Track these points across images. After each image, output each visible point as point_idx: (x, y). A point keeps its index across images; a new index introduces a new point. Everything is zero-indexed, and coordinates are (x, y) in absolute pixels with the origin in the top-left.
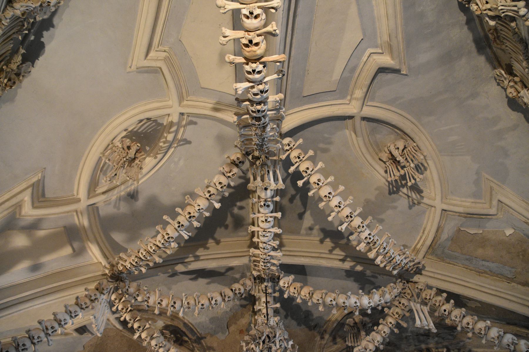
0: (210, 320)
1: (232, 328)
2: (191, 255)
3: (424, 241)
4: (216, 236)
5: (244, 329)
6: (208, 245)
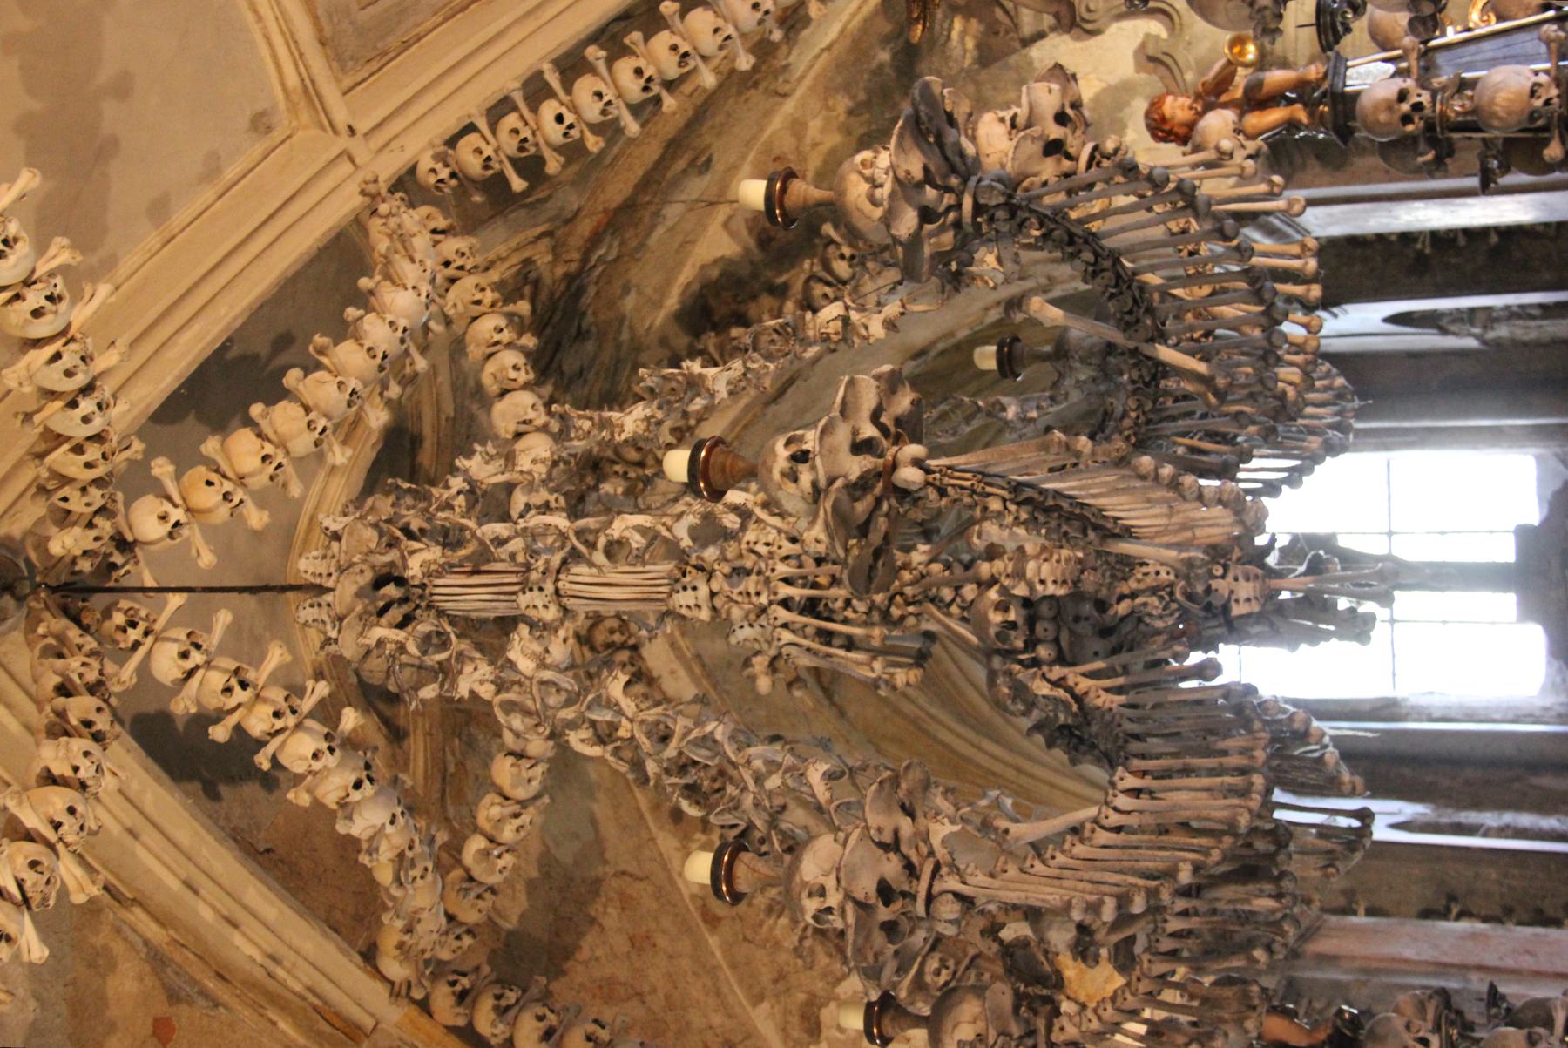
3: (292, 40)
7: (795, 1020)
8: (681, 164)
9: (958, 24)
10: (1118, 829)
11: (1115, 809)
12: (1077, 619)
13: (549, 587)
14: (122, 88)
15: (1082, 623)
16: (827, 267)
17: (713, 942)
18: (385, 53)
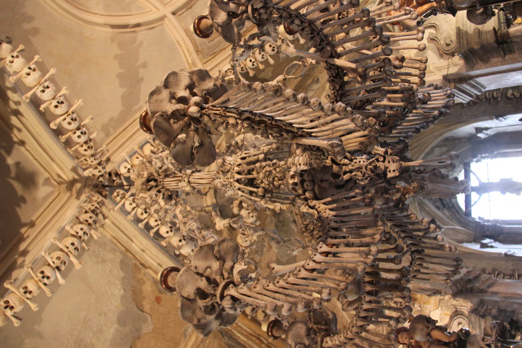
0: (119, 324)
1: (147, 307)
2: (16, 257)
3: (188, 51)
4: (24, 219)
5: (157, 294)
6: (25, 236)
8: (310, 81)
10: (313, 270)
11: (314, 261)
12: (322, 181)
13: (186, 180)
14: (145, 65)
15: (325, 183)
18: (215, 53)
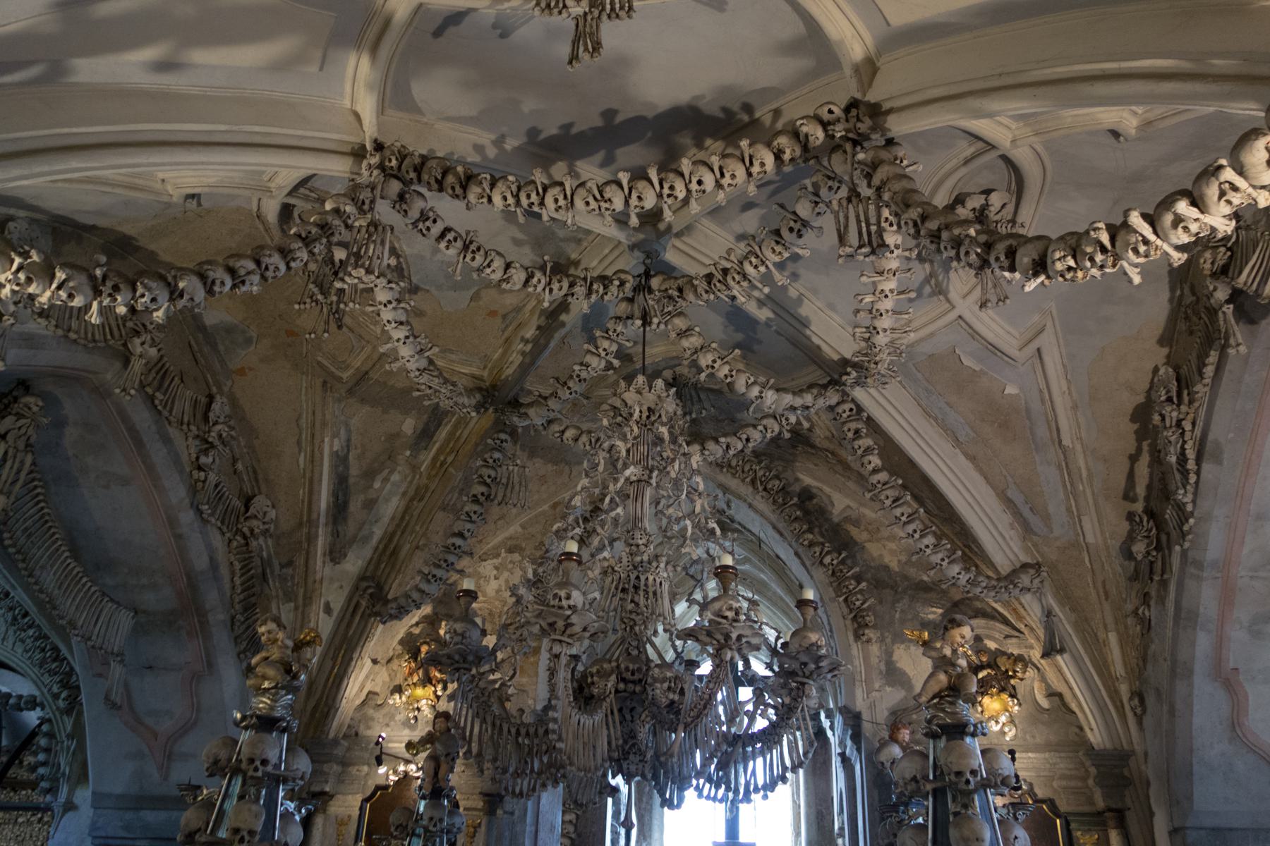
7: (514, 542)
9: (940, 611)
16: (828, 553)
17: (546, 507)
